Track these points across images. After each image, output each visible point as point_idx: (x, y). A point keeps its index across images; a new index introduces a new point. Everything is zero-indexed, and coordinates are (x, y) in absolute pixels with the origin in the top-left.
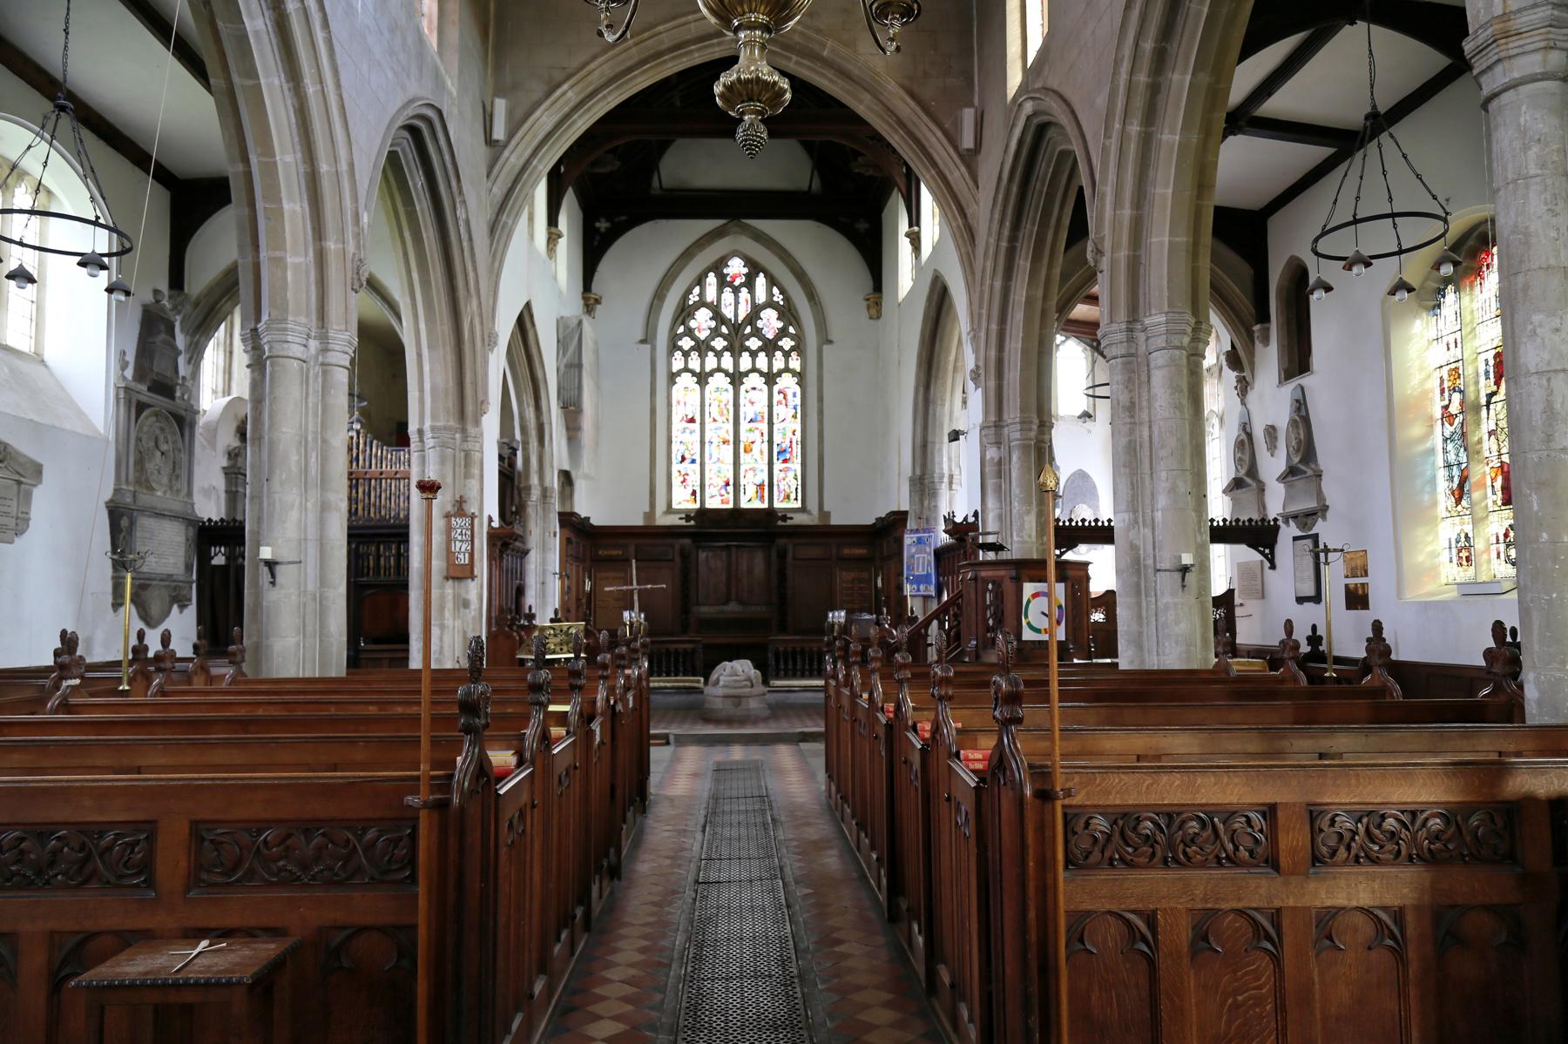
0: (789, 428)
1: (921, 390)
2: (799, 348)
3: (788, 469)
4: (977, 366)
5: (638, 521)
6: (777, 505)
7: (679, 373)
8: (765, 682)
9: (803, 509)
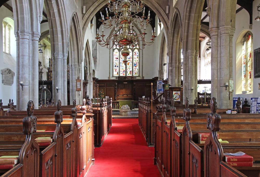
0: (136, 60)
1: (161, 54)
2: (139, 44)
4: (168, 53)
5: (107, 79)
6: (134, 75)
7: (115, 49)
8: (131, 109)
9: (139, 76)
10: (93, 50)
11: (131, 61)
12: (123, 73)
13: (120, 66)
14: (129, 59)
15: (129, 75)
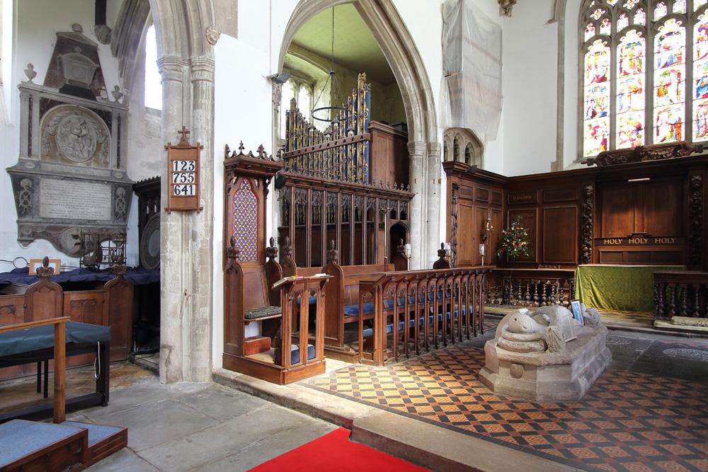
5: (546, 169)
7: (590, 42)
10: (446, 42)
11: (679, 75)
12: (634, 136)
13: (618, 112)
14: (666, 65)
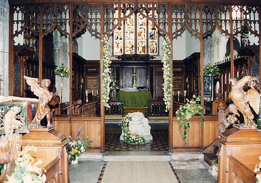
3: (153, 41)
6: (149, 54)
12: (131, 49)
13: (126, 39)
14: (141, 25)
15: (140, 51)
